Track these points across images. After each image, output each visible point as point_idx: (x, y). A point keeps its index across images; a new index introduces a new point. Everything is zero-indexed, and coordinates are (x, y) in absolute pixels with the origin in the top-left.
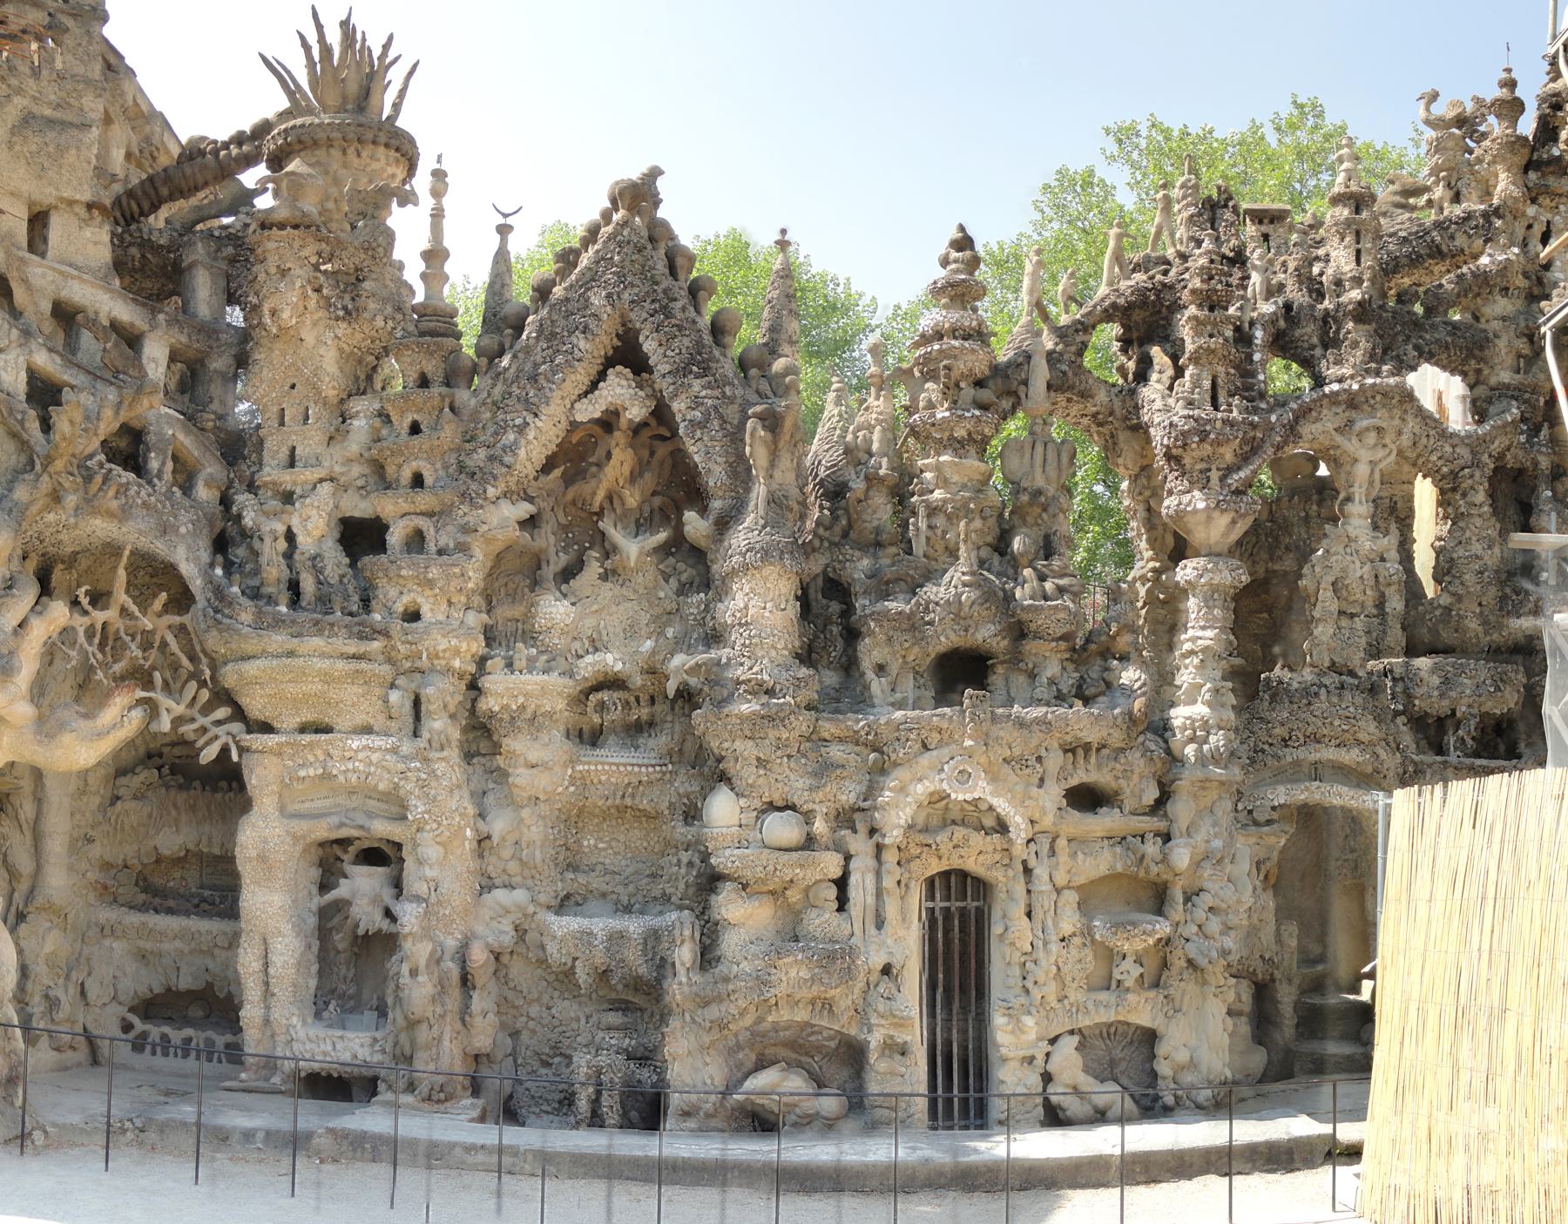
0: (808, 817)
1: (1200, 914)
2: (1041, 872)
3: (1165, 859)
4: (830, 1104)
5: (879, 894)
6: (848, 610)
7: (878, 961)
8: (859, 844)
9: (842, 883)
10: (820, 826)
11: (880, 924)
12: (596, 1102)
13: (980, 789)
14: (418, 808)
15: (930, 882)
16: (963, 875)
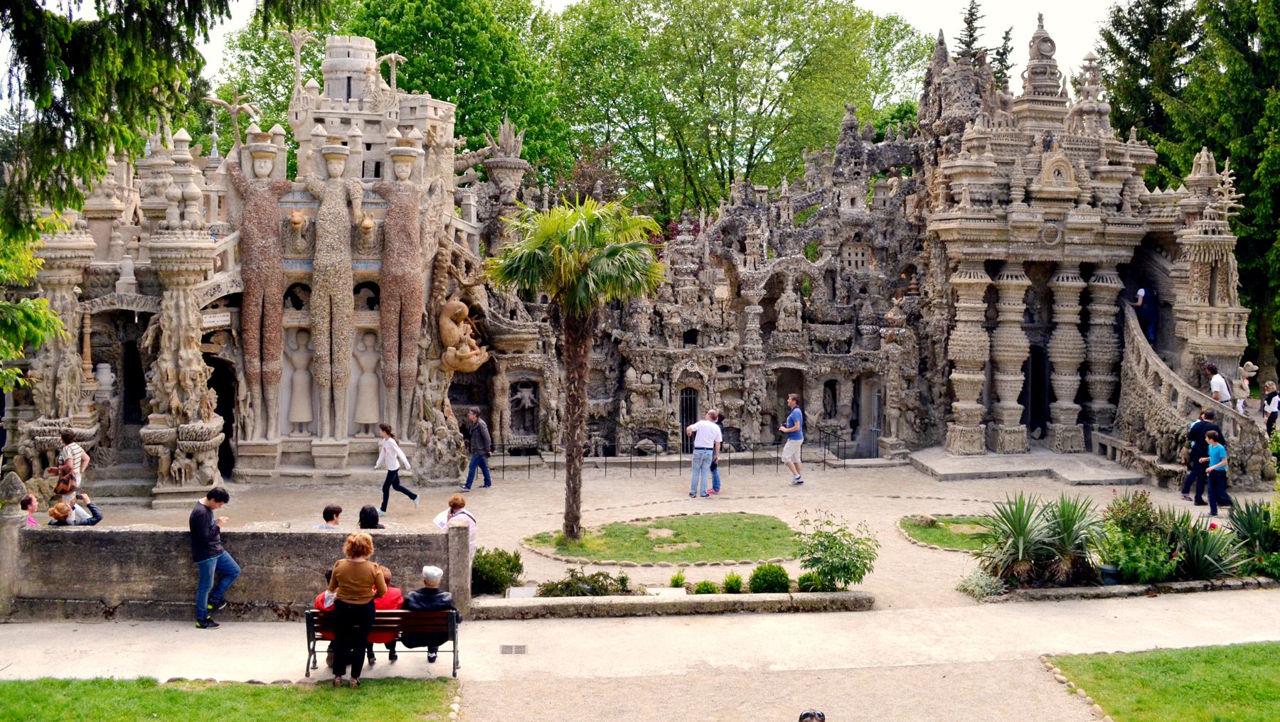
0: (653, 375)
1: (752, 399)
2: (711, 388)
3: (743, 384)
4: (660, 448)
5: (671, 394)
6: (661, 320)
7: (670, 411)
8: (666, 382)
9: (661, 392)
10: (656, 377)
11: (670, 401)
12: (596, 449)
13: (696, 368)
14: (548, 374)
15: (682, 391)
16: (691, 389)
